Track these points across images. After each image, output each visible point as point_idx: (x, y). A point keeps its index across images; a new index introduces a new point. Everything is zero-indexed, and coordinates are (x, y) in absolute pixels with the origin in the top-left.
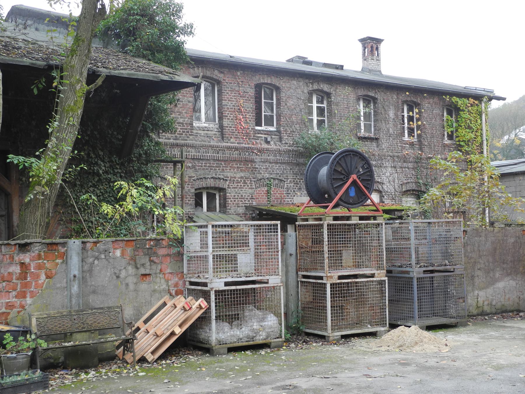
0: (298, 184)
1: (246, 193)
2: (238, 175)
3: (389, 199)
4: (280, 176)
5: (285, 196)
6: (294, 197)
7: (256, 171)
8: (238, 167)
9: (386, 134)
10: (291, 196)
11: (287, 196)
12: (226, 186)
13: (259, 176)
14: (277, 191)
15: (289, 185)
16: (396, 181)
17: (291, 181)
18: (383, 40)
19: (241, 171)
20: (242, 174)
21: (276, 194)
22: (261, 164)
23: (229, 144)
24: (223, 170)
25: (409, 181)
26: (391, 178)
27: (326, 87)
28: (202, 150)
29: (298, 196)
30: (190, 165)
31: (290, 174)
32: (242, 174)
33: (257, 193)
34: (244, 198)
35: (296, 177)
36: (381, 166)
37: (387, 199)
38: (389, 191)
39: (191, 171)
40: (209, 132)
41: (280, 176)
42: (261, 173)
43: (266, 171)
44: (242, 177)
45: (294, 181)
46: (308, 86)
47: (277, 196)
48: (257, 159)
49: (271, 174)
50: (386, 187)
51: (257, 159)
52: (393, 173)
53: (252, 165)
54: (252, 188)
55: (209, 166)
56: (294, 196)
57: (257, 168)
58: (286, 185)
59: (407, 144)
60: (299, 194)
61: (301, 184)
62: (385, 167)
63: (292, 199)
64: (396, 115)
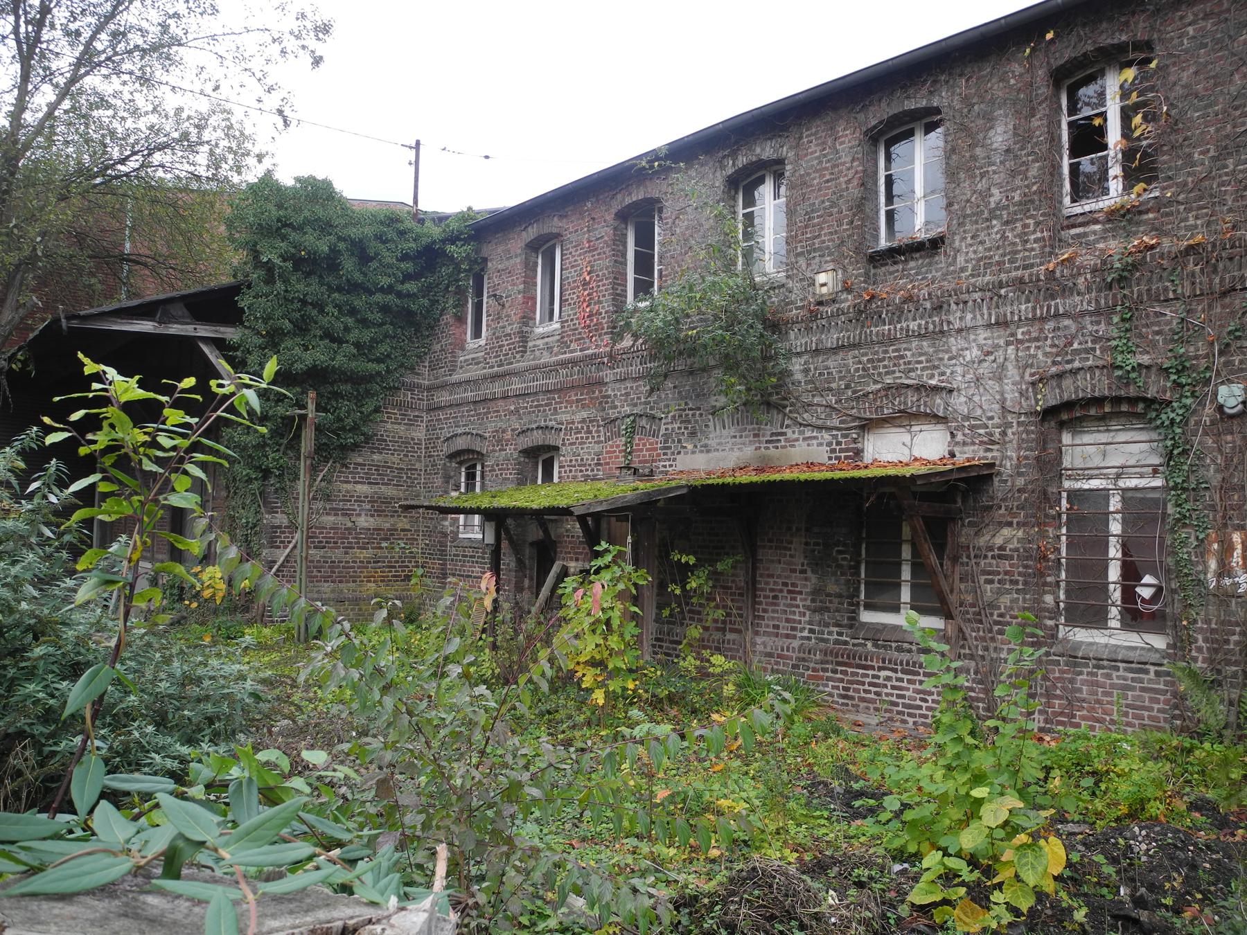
0: (689, 422)
1: (589, 453)
2: (578, 417)
3: (973, 443)
4: (652, 409)
5: (659, 455)
6: (678, 457)
7: (607, 403)
8: (578, 401)
9: (973, 214)
10: (673, 453)
11: (665, 454)
12: (559, 443)
13: (613, 414)
14: (644, 445)
15: (670, 427)
16: (1012, 371)
17: (674, 417)
20: (584, 414)
21: (641, 450)
22: (618, 385)
23: (567, 355)
24: (555, 409)
25: (1077, 364)
26: (985, 369)
27: (766, 150)
29: (686, 453)
30: (512, 408)
31: (673, 399)
32: (584, 414)
33: (607, 452)
34: (584, 465)
35: (686, 404)
36: (942, 332)
37: (965, 444)
38: (979, 412)
39: (514, 418)
40: (550, 339)
41: (652, 409)
42: (616, 407)
43: (626, 401)
44: (583, 421)
45: (680, 416)
46: (723, 168)
47: (644, 456)
48: (608, 375)
49: (635, 405)
50: (963, 399)
51: (608, 375)
52: (997, 347)
53: (601, 392)
54: (599, 442)
55: (536, 406)
56: (679, 453)
57: (609, 396)
58: (663, 427)
59: (1096, 222)
60: (690, 447)
61: (696, 422)
62: (960, 331)
63: (674, 460)
64: (1022, 136)
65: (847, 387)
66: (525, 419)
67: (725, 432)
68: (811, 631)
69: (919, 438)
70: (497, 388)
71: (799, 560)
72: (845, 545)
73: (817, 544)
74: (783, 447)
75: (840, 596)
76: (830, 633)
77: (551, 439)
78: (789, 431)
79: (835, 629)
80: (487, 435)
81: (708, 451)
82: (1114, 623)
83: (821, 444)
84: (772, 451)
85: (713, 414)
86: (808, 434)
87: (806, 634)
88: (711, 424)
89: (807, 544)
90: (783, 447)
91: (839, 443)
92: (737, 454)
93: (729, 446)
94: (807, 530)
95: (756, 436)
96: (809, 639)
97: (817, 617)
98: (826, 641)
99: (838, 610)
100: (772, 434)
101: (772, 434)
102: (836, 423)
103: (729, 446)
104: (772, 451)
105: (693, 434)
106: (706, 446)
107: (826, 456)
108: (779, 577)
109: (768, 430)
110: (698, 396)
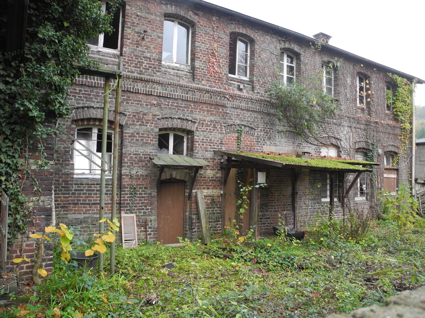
0: (268, 133)
1: (216, 138)
2: (208, 119)
4: (250, 124)
5: (255, 144)
6: (264, 146)
7: (227, 116)
8: (208, 111)
10: (261, 144)
11: (257, 144)
12: (194, 129)
14: (247, 139)
15: (259, 133)
16: (351, 139)
17: (261, 130)
18: (331, 37)
19: (212, 114)
21: (246, 141)
22: (233, 110)
23: (200, 86)
24: (192, 111)
25: (361, 140)
27: (296, 48)
28: (169, 88)
29: (267, 145)
30: (155, 102)
31: (261, 123)
32: (213, 118)
33: (227, 139)
34: (213, 143)
35: (267, 126)
36: (340, 125)
38: (345, 147)
40: (180, 72)
41: (250, 124)
42: (232, 119)
43: (237, 118)
44: (212, 121)
45: (264, 130)
47: (247, 143)
48: (229, 104)
49: (243, 121)
51: (229, 104)
52: (349, 132)
53: (223, 110)
54: (222, 133)
55: (176, 106)
56: (264, 145)
57: (229, 114)
58: (256, 133)
61: (271, 134)
62: (343, 126)
63: (262, 147)
65: (319, 134)
66: (165, 111)
67: (282, 140)
68: (312, 206)
69: (330, 151)
70: (140, 86)
71: (307, 184)
72: (319, 180)
73: (312, 180)
74: (302, 148)
75: (318, 195)
76: (316, 206)
77: (189, 126)
78: (303, 144)
79: (317, 205)
80: (128, 114)
81: (276, 146)
82: (359, 196)
83: (312, 149)
84: (298, 149)
85: (278, 132)
86: (309, 145)
87: (310, 207)
88: (277, 136)
89: (309, 179)
90: (302, 148)
91: (317, 150)
92: (287, 148)
93: (284, 145)
94: (309, 175)
95: (293, 143)
96: (311, 209)
97: (313, 202)
98: (315, 208)
99: (318, 199)
100: (299, 144)
101: (299, 144)
102: (316, 144)
103: (284, 145)
104: (298, 149)
105: (269, 138)
106: (275, 144)
107: (314, 153)
108: (302, 190)
109: (297, 142)
110: (272, 124)
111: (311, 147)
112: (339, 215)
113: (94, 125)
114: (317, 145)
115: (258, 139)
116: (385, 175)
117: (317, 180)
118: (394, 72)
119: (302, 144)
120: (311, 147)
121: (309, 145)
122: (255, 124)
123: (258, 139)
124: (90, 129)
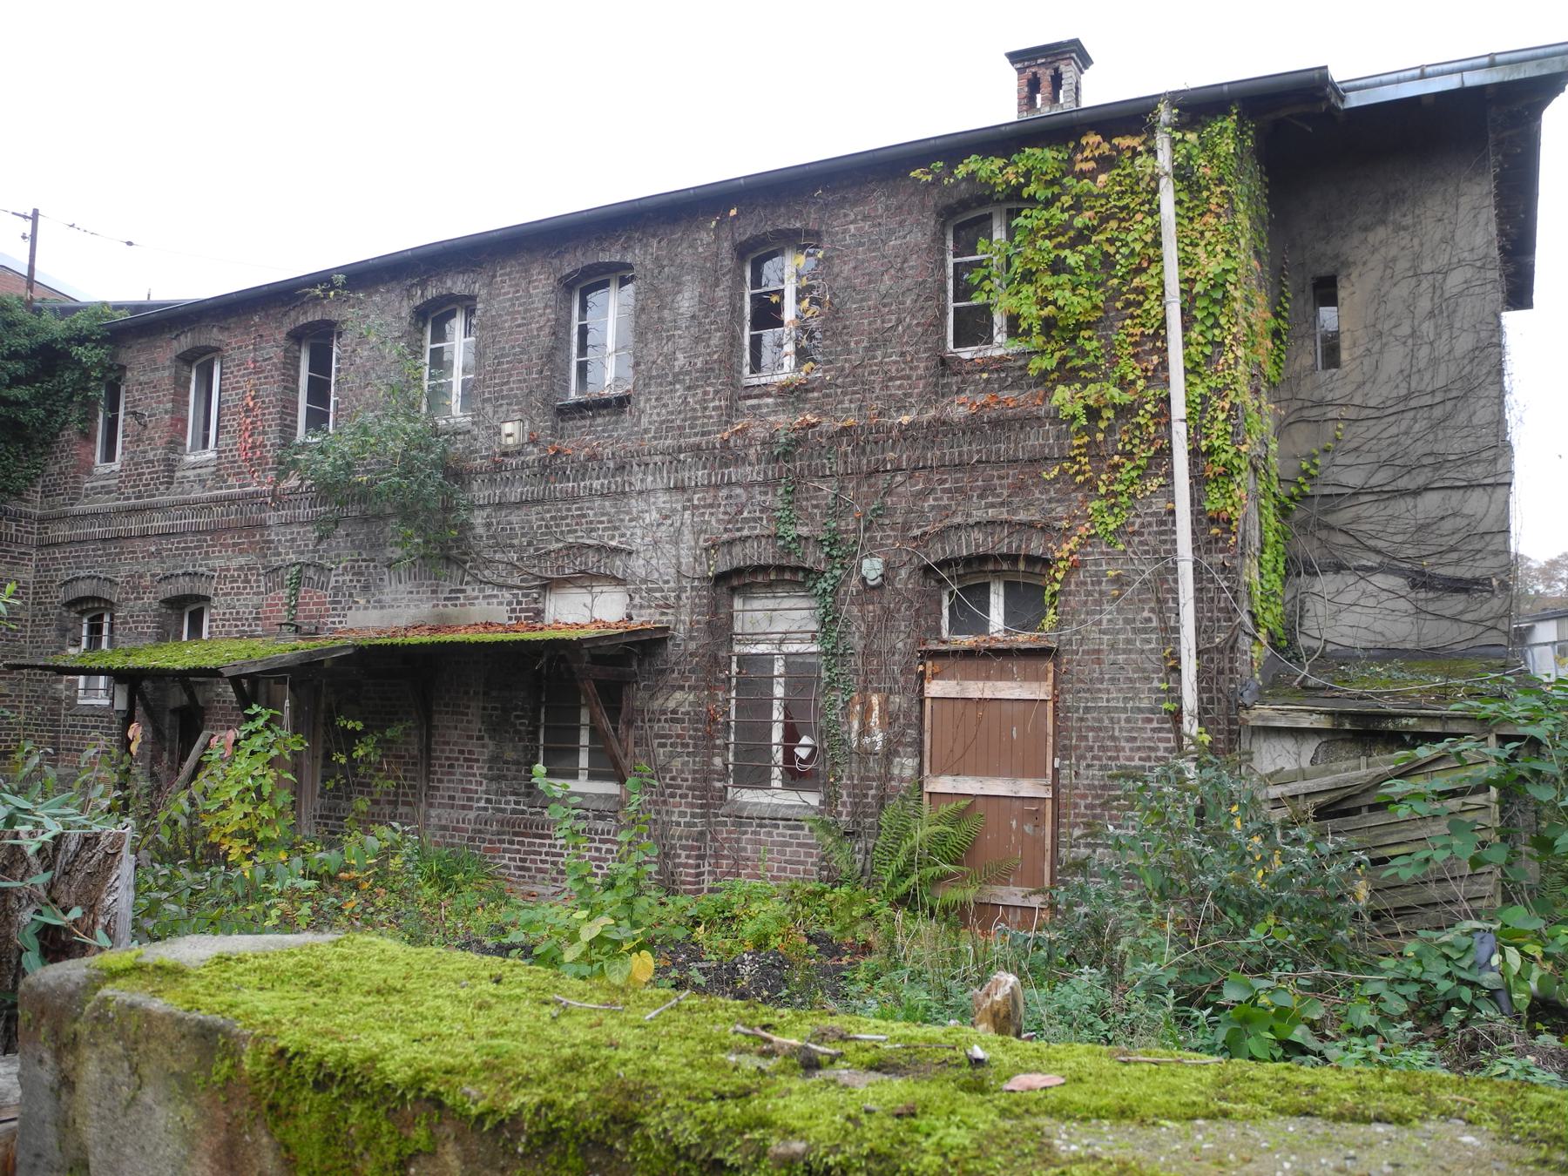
0: (362, 574)
1: (247, 606)
2: (234, 564)
3: (650, 607)
4: (320, 558)
5: (327, 610)
8: (234, 545)
9: (658, 376)
13: (275, 561)
16: (687, 536)
18: (1015, 57)
19: (241, 552)
20: (242, 560)
22: (282, 529)
23: (224, 491)
24: (207, 553)
25: (746, 532)
26: (663, 533)
27: (457, 285)
28: (175, 513)
30: (153, 549)
32: (242, 560)
36: (624, 493)
37: (641, 607)
39: (154, 561)
41: (320, 558)
42: (279, 554)
44: (241, 568)
46: (410, 297)
48: (272, 517)
49: (302, 553)
50: (641, 562)
51: (272, 517)
52: (674, 511)
57: (272, 542)
58: (333, 579)
59: (769, 395)
60: (362, 602)
62: (641, 493)
64: (707, 304)
65: (530, 544)
66: (169, 563)
67: (401, 587)
68: (488, 801)
69: (600, 600)
70: (134, 525)
71: (477, 726)
72: (523, 709)
73: (494, 709)
74: (462, 605)
75: (517, 763)
76: (507, 803)
77: (200, 588)
78: (469, 588)
79: (512, 798)
80: (119, 580)
81: (382, 608)
82: (776, 783)
83: (501, 603)
84: (450, 609)
85: (389, 567)
86: (488, 592)
87: (482, 804)
88: (386, 577)
89: (484, 708)
90: (462, 605)
91: (519, 603)
92: (413, 611)
93: (405, 602)
94: (485, 694)
95: (434, 592)
96: (486, 809)
97: (494, 786)
98: (503, 811)
99: (515, 778)
100: (451, 591)
101: (451, 591)
102: (516, 581)
103: (405, 602)
104: (450, 609)
105: (366, 588)
106: (379, 601)
107: (506, 616)
108: (455, 744)
109: (447, 586)
110: (372, 546)
111: (496, 596)
112: (598, 850)
113: (997, 573)
114: (519, 588)
115: (336, 595)
116: (934, 688)
117: (515, 709)
118: (954, 149)
119: (463, 591)
120: (496, 596)
121: (488, 592)
122: (332, 554)
123: (336, 595)
124: (985, 589)
